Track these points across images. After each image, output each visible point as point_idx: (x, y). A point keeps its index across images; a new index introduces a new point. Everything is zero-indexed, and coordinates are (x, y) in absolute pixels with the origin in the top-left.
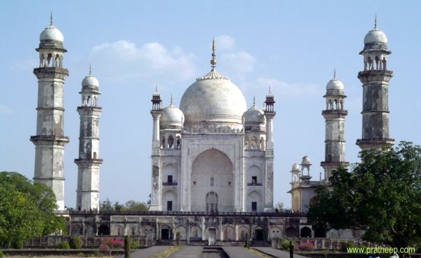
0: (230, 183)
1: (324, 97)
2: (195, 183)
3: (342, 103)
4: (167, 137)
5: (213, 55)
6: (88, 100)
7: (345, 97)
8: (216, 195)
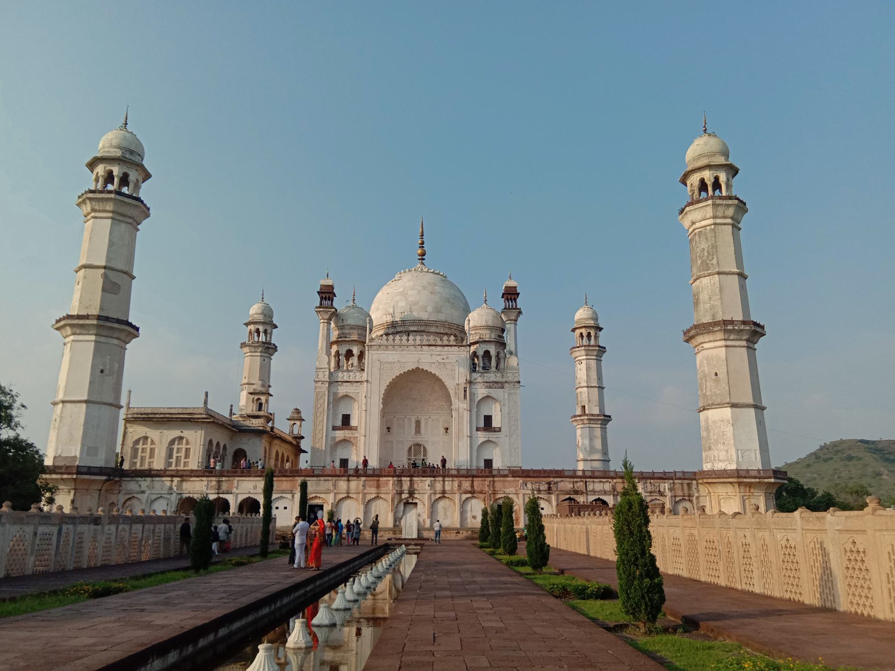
3: (596, 337)
4: (343, 350)
5: (423, 243)
7: (601, 329)
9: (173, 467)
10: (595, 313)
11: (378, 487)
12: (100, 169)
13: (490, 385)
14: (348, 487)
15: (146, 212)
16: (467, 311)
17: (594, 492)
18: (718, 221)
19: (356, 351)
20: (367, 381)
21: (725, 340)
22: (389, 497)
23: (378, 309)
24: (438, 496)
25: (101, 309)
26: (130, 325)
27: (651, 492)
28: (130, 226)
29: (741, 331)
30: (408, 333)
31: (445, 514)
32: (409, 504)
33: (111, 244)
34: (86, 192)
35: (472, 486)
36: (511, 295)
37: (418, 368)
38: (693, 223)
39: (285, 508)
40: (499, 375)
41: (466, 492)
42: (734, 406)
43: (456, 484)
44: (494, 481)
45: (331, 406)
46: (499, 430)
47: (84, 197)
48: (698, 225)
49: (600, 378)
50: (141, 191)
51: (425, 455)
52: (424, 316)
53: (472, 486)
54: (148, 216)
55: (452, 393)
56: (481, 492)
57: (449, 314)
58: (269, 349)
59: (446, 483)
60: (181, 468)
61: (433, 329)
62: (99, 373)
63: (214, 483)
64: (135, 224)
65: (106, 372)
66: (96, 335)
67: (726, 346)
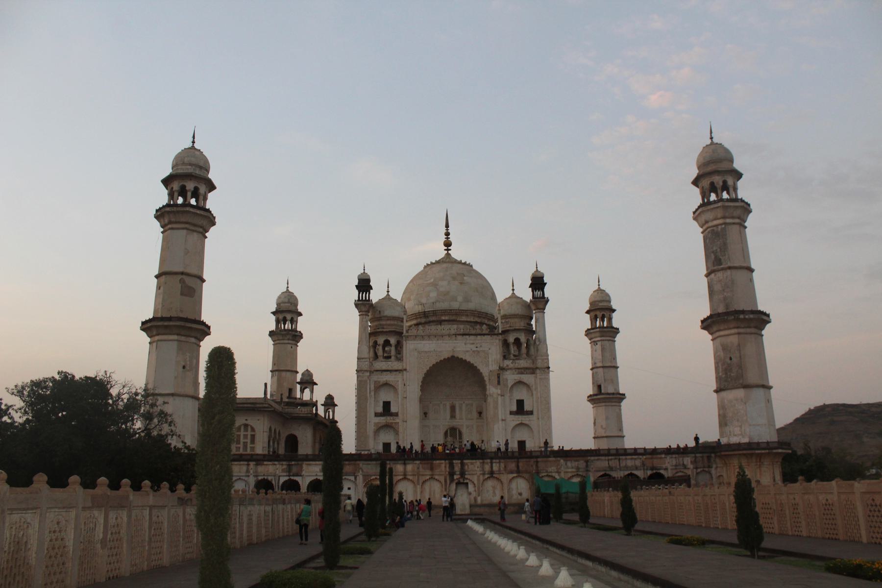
0: (480, 413)
1: (588, 312)
2: (425, 414)
3: (610, 319)
4: (381, 340)
5: (447, 234)
6: (285, 324)
7: (614, 311)
8: (460, 433)
9: (241, 451)
10: (608, 295)
11: (432, 469)
12: (176, 186)
14: (405, 469)
15: (212, 221)
17: (627, 468)
18: (728, 221)
19: (393, 341)
20: (405, 370)
21: (738, 328)
22: (442, 479)
23: (409, 299)
24: (486, 476)
25: (182, 311)
26: (203, 323)
27: (676, 466)
28: (201, 235)
29: (751, 319)
30: (440, 322)
31: (494, 492)
32: (462, 483)
33: (187, 252)
34: (164, 207)
35: (518, 467)
37: (453, 357)
38: (707, 222)
39: (349, 489)
40: (530, 361)
41: (512, 472)
42: (746, 387)
43: (502, 465)
44: (537, 462)
45: (373, 393)
46: (531, 413)
47: (163, 210)
48: (710, 224)
49: (615, 358)
50: (208, 202)
51: (461, 438)
52: (455, 305)
53: (518, 467)
54: (214, 224)
55: (486, 379)
56: (526, 472)
58: (296, 336)
59: (494, 465)
60: (249, 452)
61: (464, 318)
62: (181, 369)
63: (285, 467)
65: (187, 368)
66: (178, 335)
67: (739, 334)
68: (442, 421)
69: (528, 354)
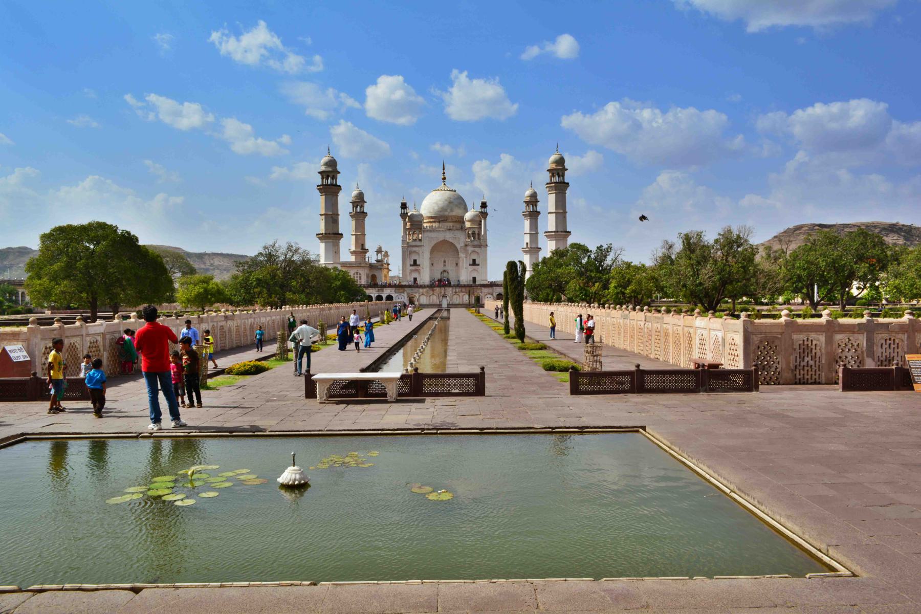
10: (535, 193)
13: (475, 246)
16: (466, 210)
32: (444, 296)
36: (484, 205)
52: (446, 214)
57: (457, 212)
64: (336, 194)
68: (439, 267)
69: (479, 239)
